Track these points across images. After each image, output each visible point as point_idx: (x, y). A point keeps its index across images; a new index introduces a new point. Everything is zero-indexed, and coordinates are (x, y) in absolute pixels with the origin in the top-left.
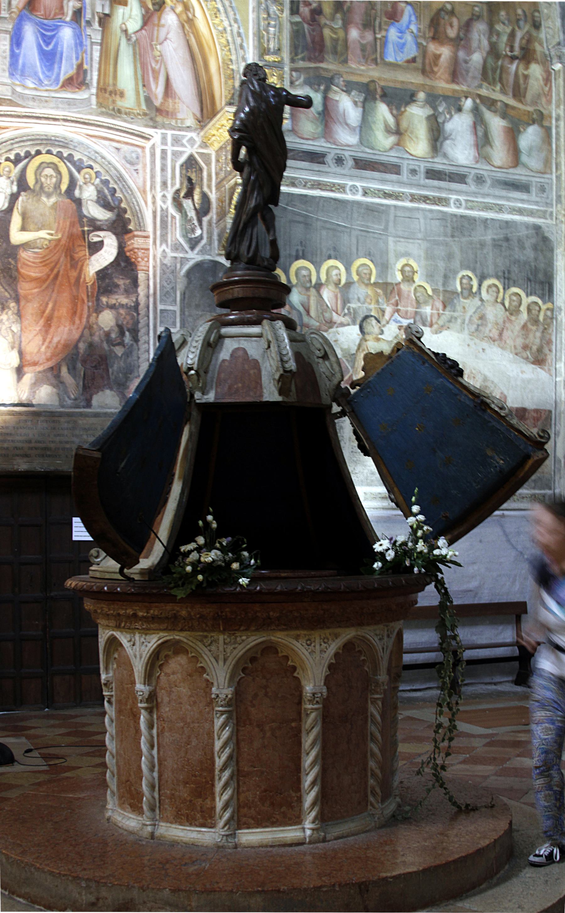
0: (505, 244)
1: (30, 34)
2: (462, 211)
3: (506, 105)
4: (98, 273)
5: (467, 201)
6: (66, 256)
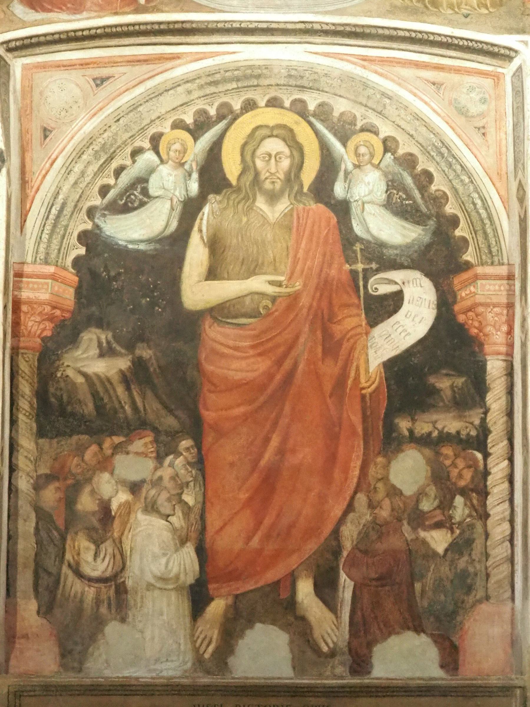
4: (390, 365)
6: (313, 331)
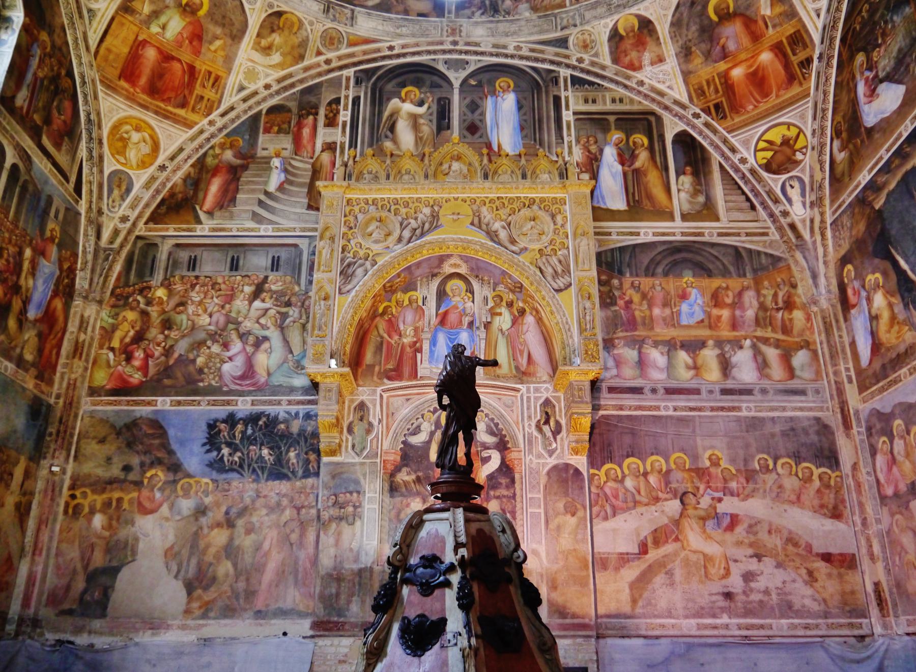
0: (791, 433)
2: (753, 414)
3: (778, 340)
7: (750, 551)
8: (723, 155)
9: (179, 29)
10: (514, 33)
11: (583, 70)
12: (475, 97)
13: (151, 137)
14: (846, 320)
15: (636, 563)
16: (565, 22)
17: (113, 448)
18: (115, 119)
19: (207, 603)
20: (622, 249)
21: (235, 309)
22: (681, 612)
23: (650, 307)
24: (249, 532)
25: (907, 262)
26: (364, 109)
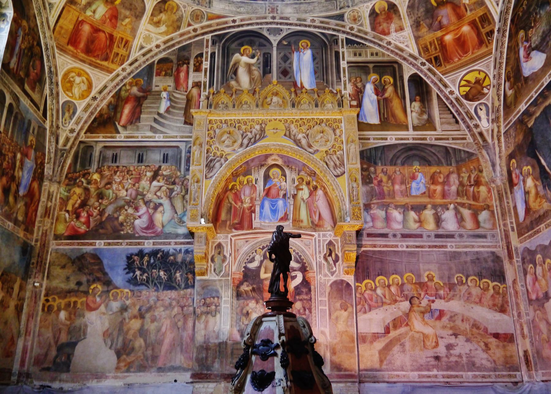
0: (477, 261)
1: (267, 204)
2: (454, 250)
3: (470, 204)
4: (295, 287)
5: (456, 245)
7: (451, 332)
8: (439, 89)
9: (104, 13)
10: (311, 11)
11: (353, 35)
12: (287, 52)
13: (87, 79)
14: (511, 193)
15: (383, 339)
16: (342, 5)
17: (70, 271)
18: (65, 69)
19: (129, 363)
20: (376, 148)
21: (141, 186)
22: (409, 368)
23: (393, 184)
24: (153, 321)
25: (545, 160)
26: (218, 60)
